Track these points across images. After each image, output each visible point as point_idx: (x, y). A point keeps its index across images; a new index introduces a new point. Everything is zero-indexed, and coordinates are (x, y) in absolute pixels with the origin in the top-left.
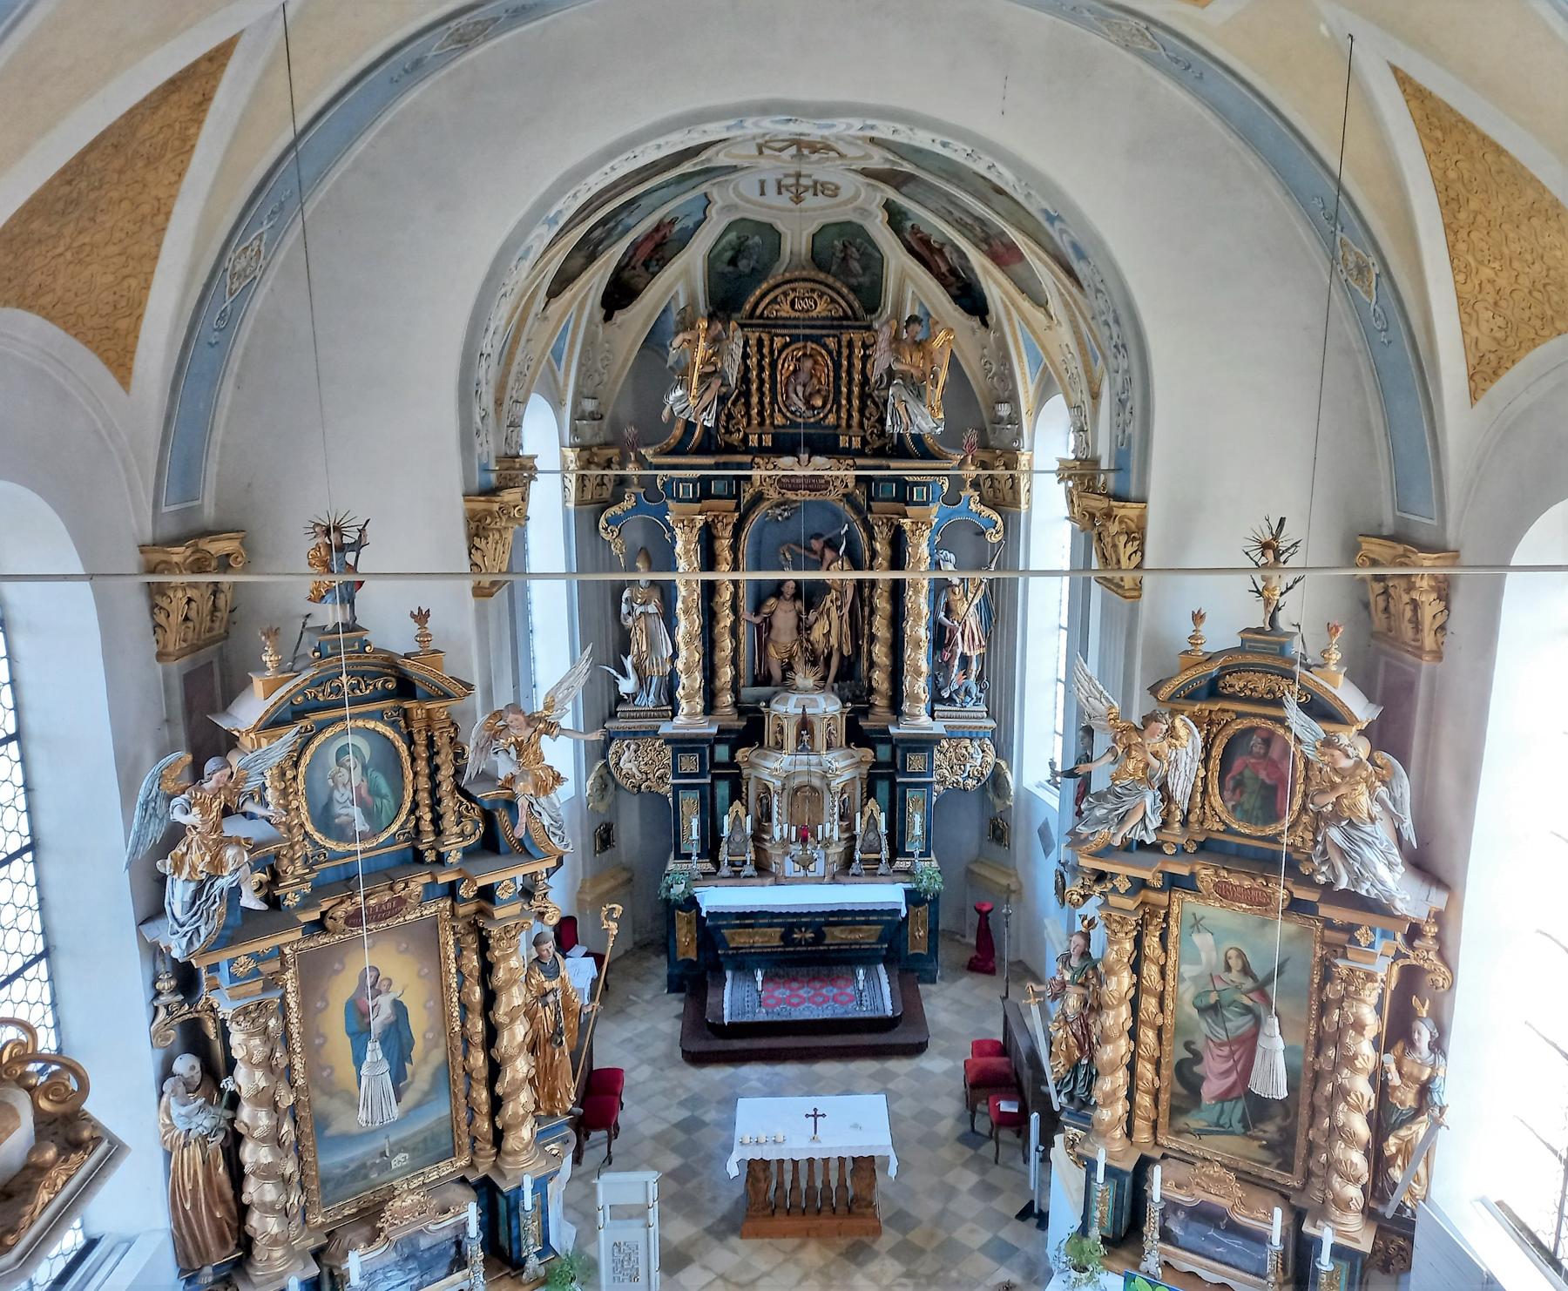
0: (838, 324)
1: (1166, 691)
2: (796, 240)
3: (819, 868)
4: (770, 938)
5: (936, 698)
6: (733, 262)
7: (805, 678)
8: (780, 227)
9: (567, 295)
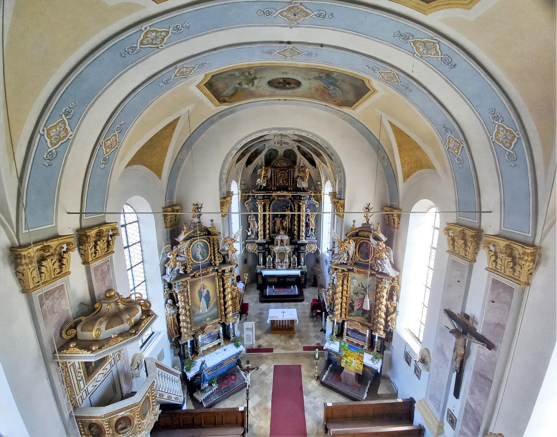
0: (289, 167)
1: (349, 235)
2: (281, 152)
3: (284, 267)
4: (275, 280)
5: (306, 236)
6: (270, 156)
7: (282, 232)
9: (239, 162)
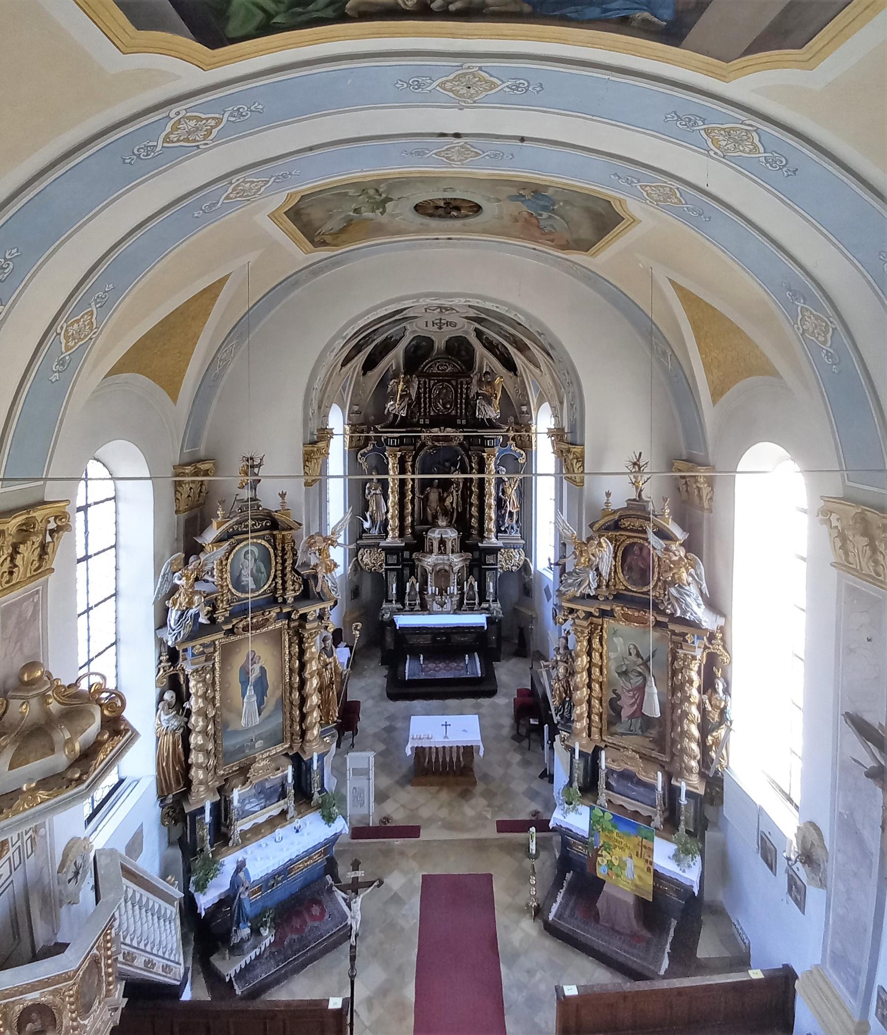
0: (455, 375)
1: (597, 526)
3: (448, 607)
4: (425, 640)
5: (499, 531)
7: (442, 522)
8: (433, 338)
9: (349, 365)
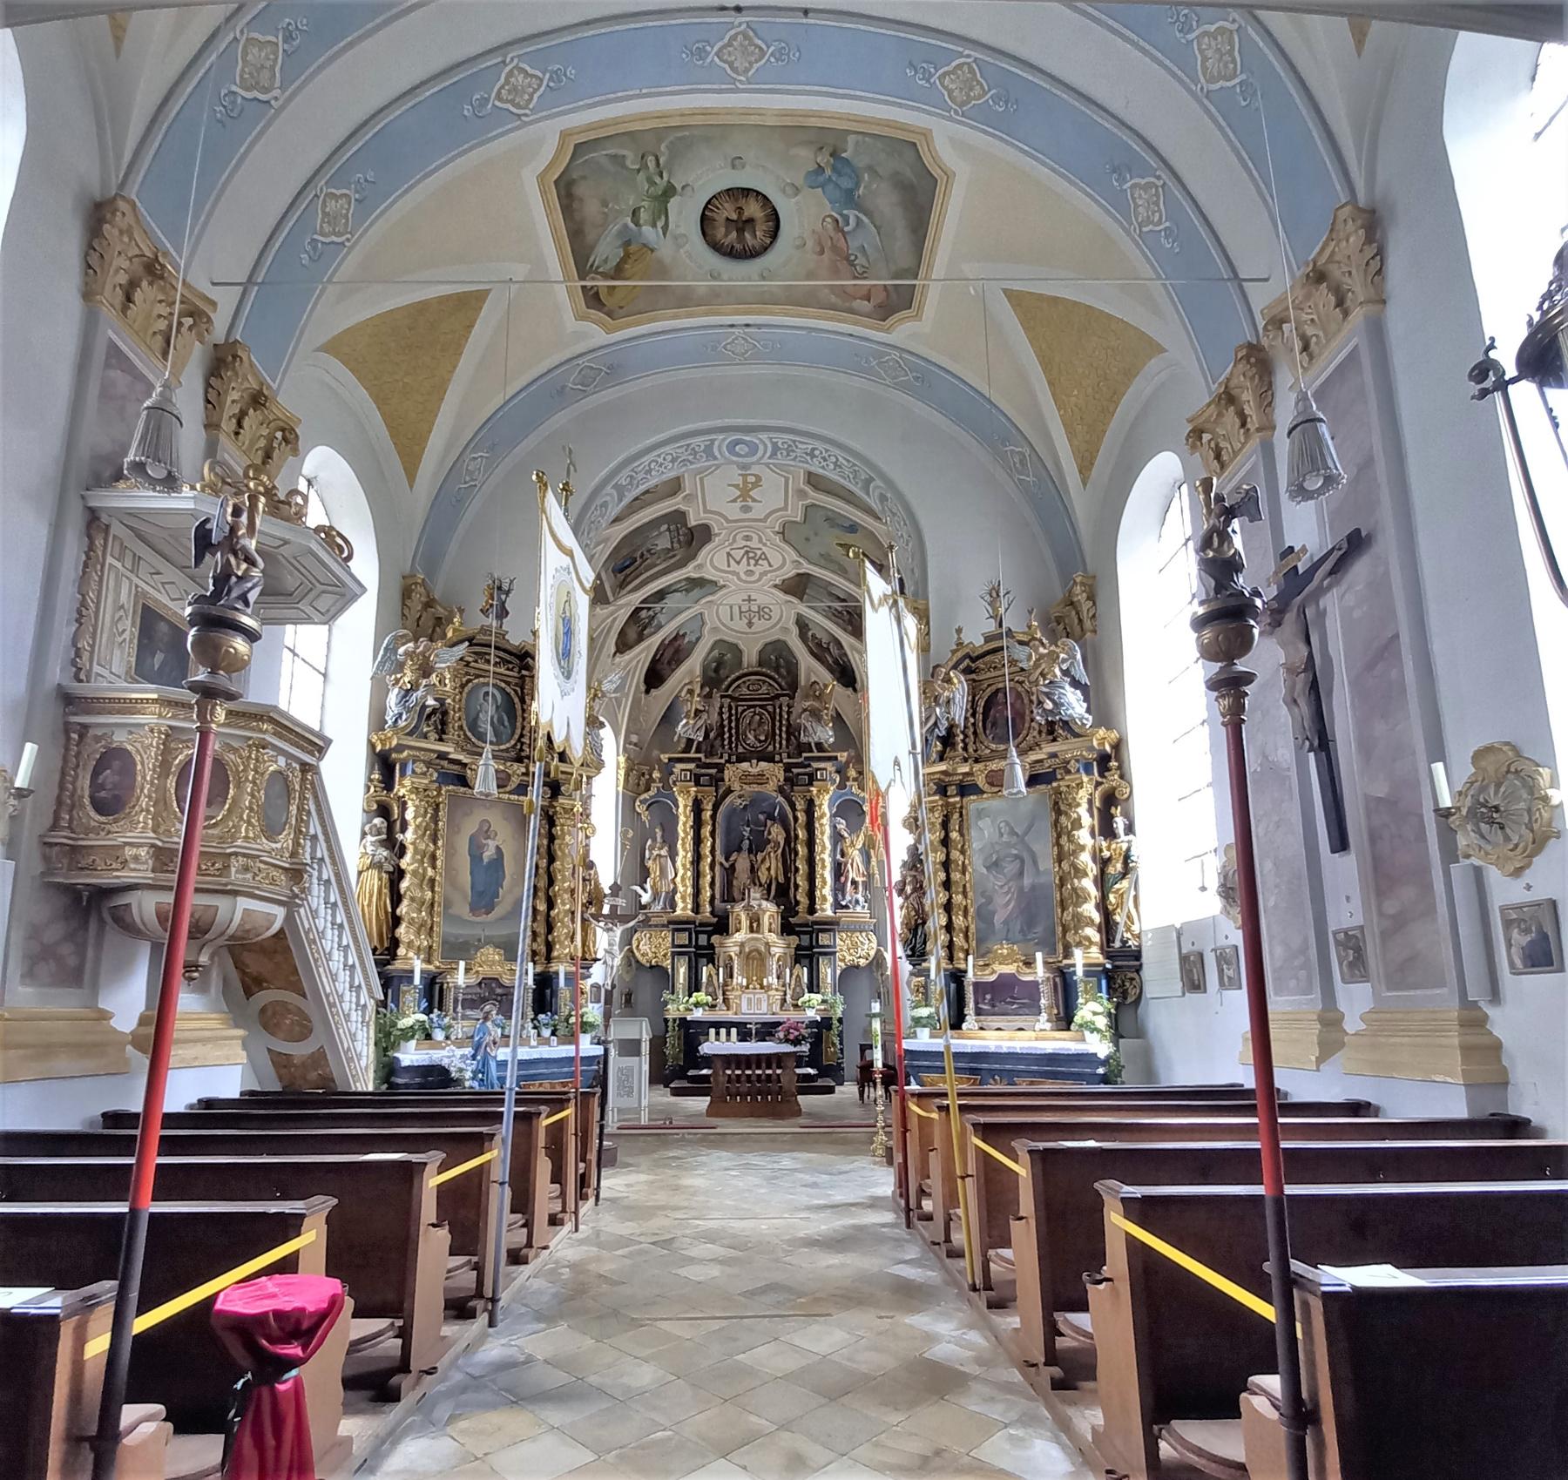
2: (750, 656)
6: (716, 670)
8: (742, 647)
